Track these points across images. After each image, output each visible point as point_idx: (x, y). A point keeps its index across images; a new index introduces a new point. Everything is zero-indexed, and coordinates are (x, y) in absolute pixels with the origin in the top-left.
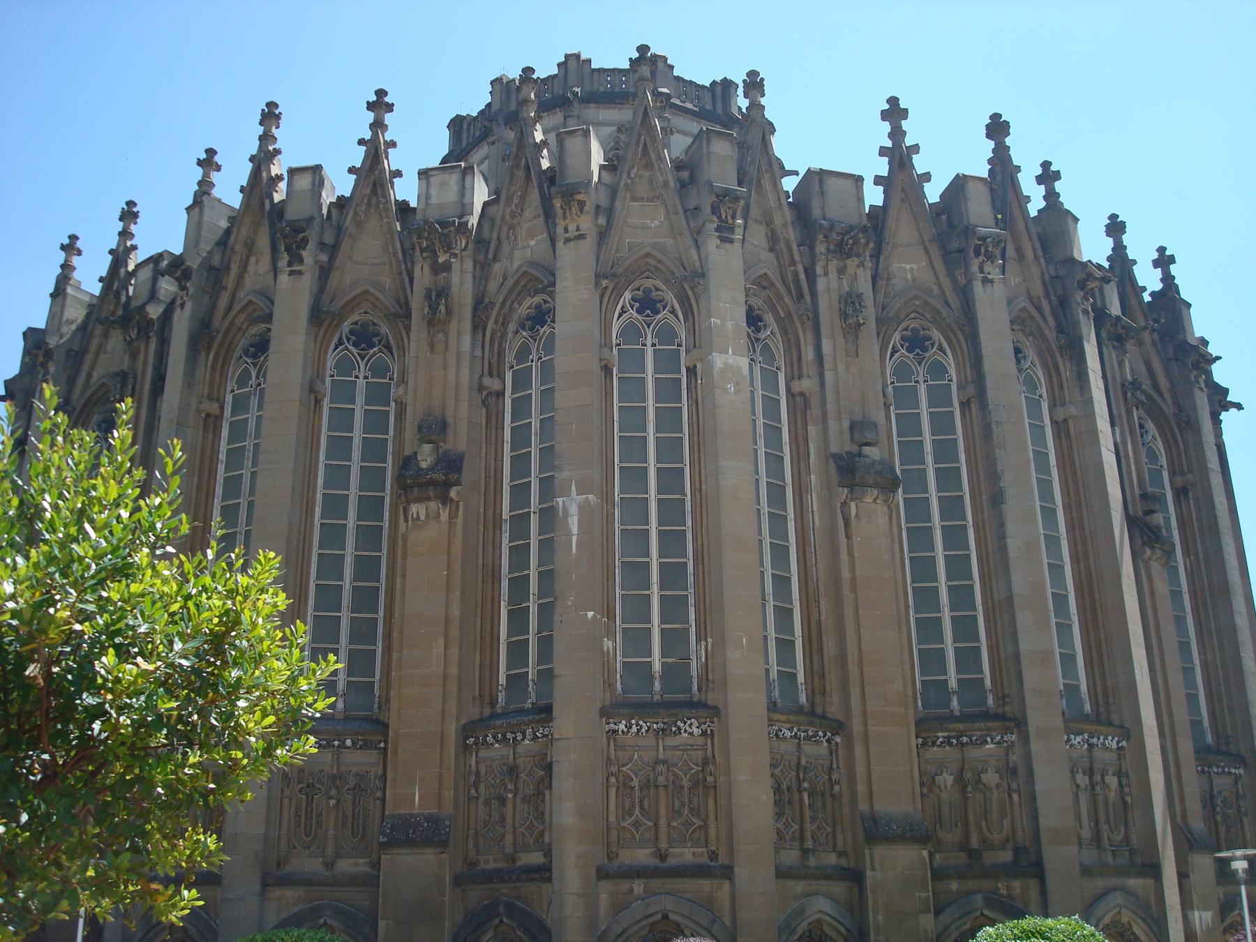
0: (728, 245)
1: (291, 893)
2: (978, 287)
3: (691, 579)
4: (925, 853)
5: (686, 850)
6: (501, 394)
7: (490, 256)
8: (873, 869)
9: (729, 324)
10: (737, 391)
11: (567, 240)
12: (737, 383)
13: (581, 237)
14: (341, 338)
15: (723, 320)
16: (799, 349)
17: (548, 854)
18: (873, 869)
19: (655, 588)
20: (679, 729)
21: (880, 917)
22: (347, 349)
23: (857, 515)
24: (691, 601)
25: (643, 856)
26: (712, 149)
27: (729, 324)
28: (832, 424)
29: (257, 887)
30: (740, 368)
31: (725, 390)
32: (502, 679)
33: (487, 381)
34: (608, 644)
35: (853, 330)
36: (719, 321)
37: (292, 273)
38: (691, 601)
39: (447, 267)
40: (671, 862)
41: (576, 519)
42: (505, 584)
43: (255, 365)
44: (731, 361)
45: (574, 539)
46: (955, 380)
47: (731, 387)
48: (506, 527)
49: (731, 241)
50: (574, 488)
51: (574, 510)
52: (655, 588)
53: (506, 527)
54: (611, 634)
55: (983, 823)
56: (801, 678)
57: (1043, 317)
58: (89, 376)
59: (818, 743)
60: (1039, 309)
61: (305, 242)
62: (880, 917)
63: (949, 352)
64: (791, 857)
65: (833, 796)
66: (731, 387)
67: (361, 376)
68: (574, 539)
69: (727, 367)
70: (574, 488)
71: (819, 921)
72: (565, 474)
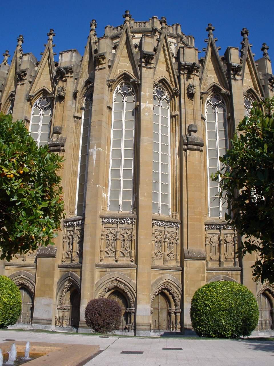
0: (149, 70)
1: (12, 268)
2: (233, 82)
4: (205, 262)
5: (124, 259)
6: (80, 118)
7: (79, 76)
8: (187, 267)
9: (148, 94)
10: (149, 115)
11: (99, 70)
12: (149, 113)
13: (103, 69)
14: (36, 104)
15: (146, 93)
18: (187, 267)
19: (122, 178)
20: (124, 221)
21: (188, 282)
22: (38, 107)
23: (189, 155)
25: (111, 261)
26: (145, 41)
27: (148, 94)
28: (183, 126)
29: (3, 266)
30: (150, 108)
31: (145, 114)
35: (191, 95)
36: (144, 93)
37: (21, 85)
39: (66, 81)
40: (119, 263)
41: (95, 156)
44: (147, 105)
45: (94, 162)
46: (226, 112)
47: (147, 114)
49: (150, 68)
50: (95, 146)
51: (95, 153)
52: (122, 178)
54: (106, 192)
55: (226, 253)
56: (170, 207)
57: (258, 92)
59: (172, 227)
60: (256, 89)
61: (25, 75)
62: (188, 282)
63: (225, 103)
64: (159, 263)
65: (176, 244)
66: (147, 114)
67: (42, 115)
68: (94, 162)
69: (146, 108)
70: (95, 146)
71: (167, 282)
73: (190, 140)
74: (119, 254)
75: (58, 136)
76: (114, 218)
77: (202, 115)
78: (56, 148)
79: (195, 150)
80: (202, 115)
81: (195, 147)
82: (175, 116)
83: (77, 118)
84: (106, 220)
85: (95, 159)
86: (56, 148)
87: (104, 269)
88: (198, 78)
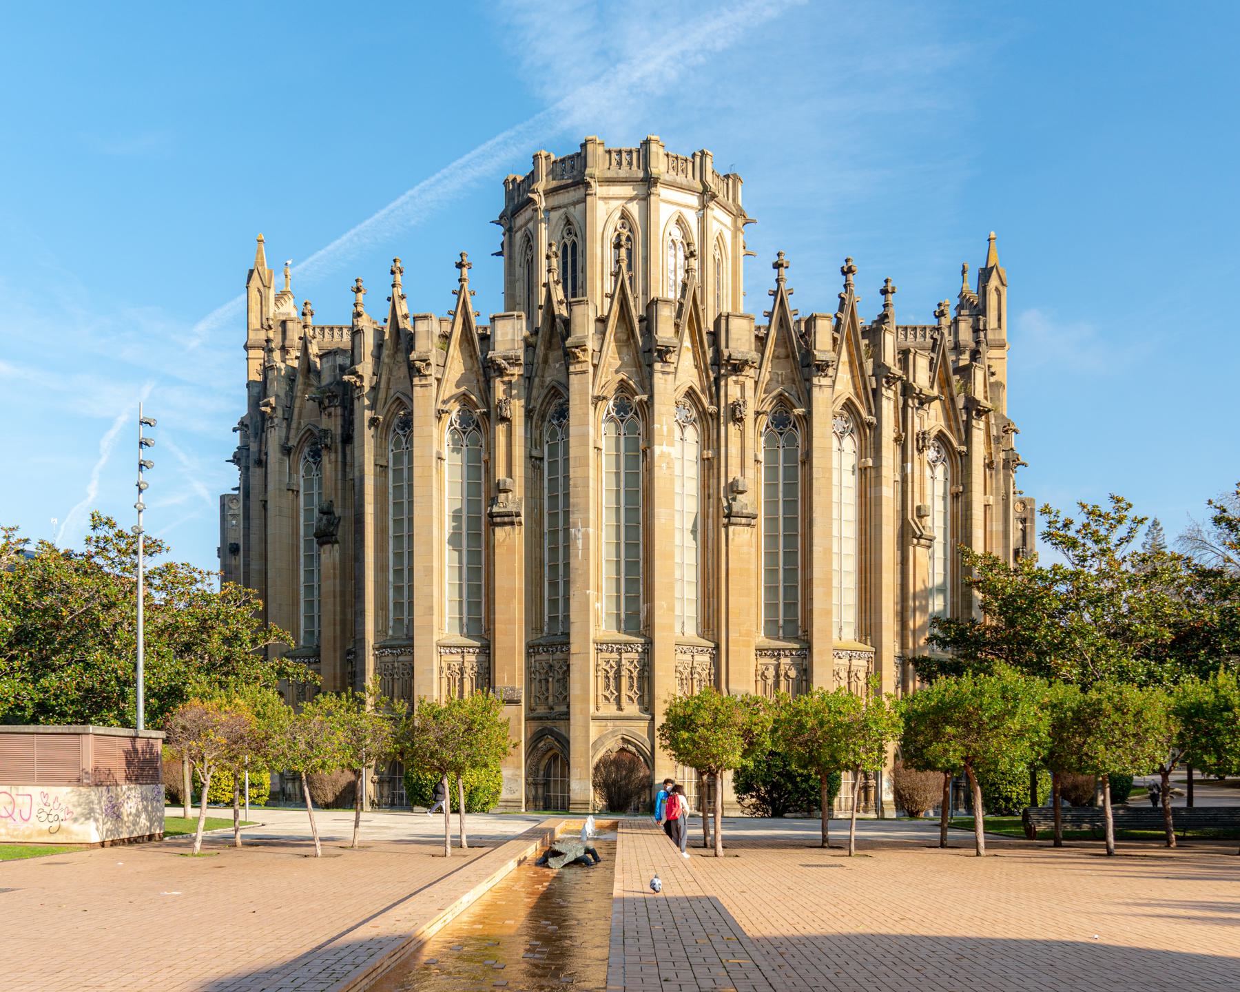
3: (641, 570)
6: (542, 459)
15: (662, 425)
16: (709, 430)
17: (568, 707)
24: (641, 582)
32: (546, 619)
33: (535, 453)
34: (598, 605)
38: (641, 582)
42: (546, 568)
43: (404, 436)
48: (546, 537)
53: (546, 537)
58: (299, 423)
69: (662, 453)
72: (576, 516)
73: (735, 509)
74: (624, 699)
75: (507, 497)
76: (615, 644)
77: (756, 455)
78: (506, 519)
79: (744, 525)
80: (756, 455)
81: (744, 521)
82: (708, 459)
83: (536, 458)
84: (604, 647)
85: (580, 546)
86: (506, 519)
87: (604, 723)
88: (753, 381)
